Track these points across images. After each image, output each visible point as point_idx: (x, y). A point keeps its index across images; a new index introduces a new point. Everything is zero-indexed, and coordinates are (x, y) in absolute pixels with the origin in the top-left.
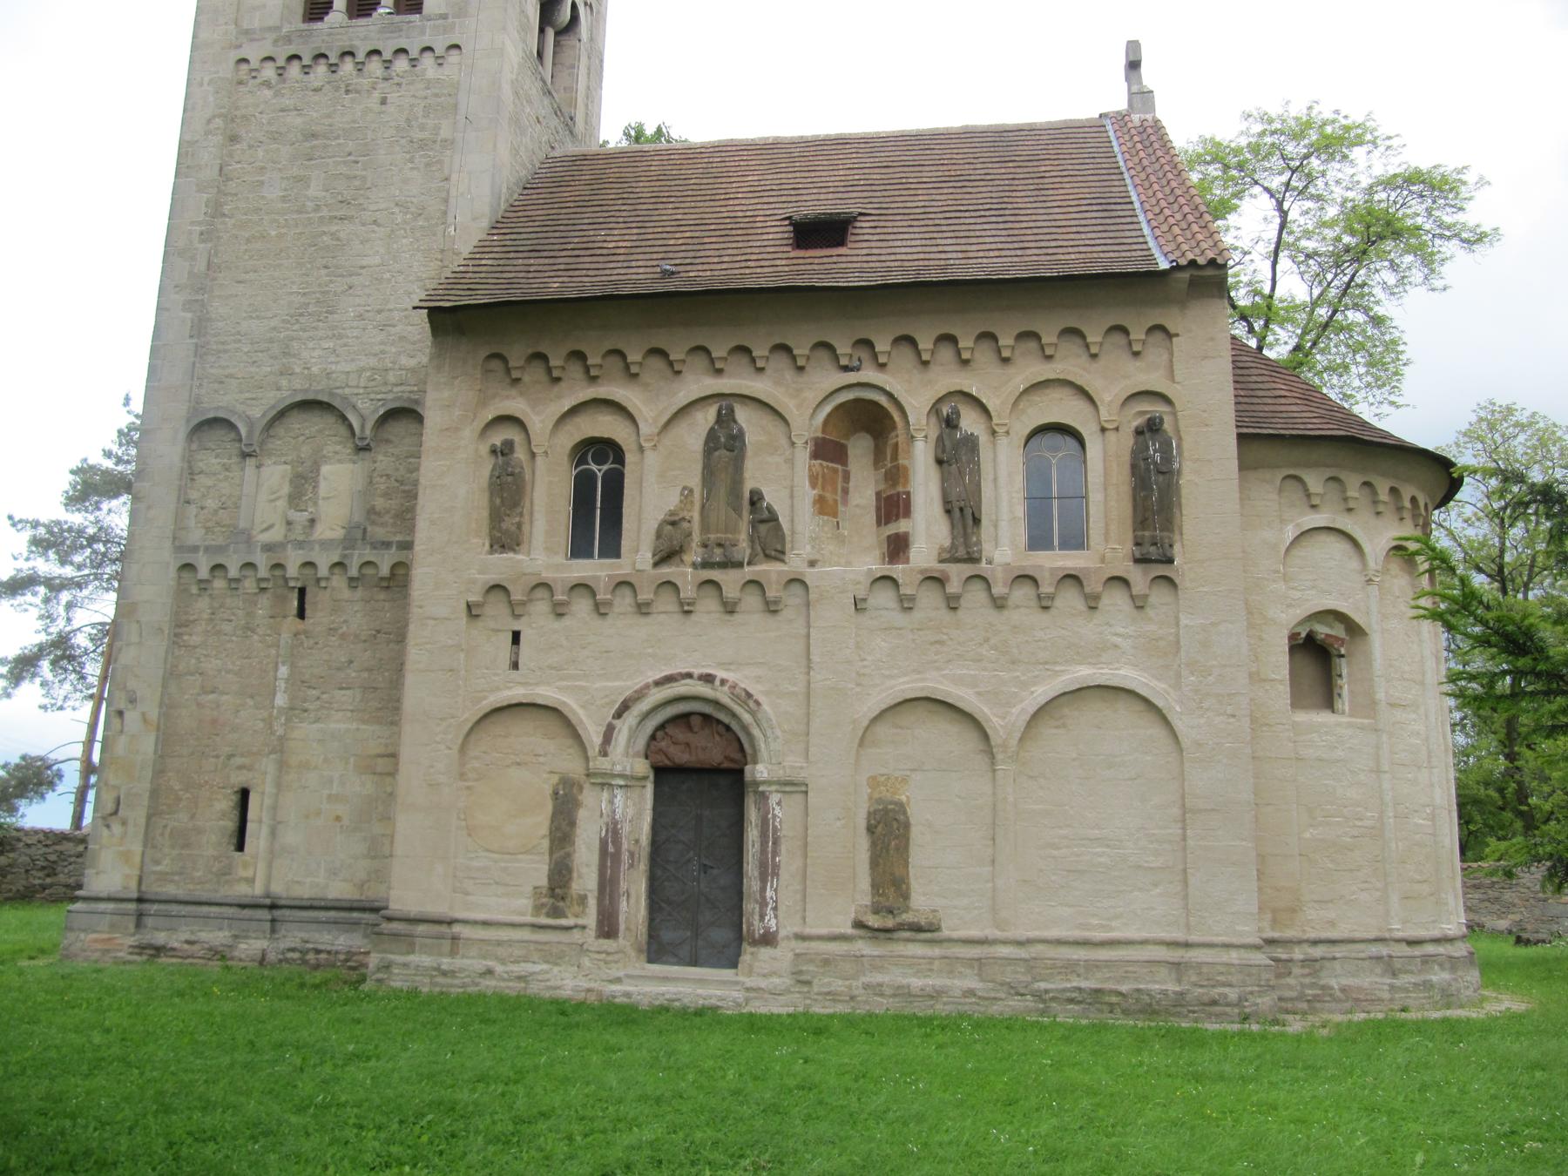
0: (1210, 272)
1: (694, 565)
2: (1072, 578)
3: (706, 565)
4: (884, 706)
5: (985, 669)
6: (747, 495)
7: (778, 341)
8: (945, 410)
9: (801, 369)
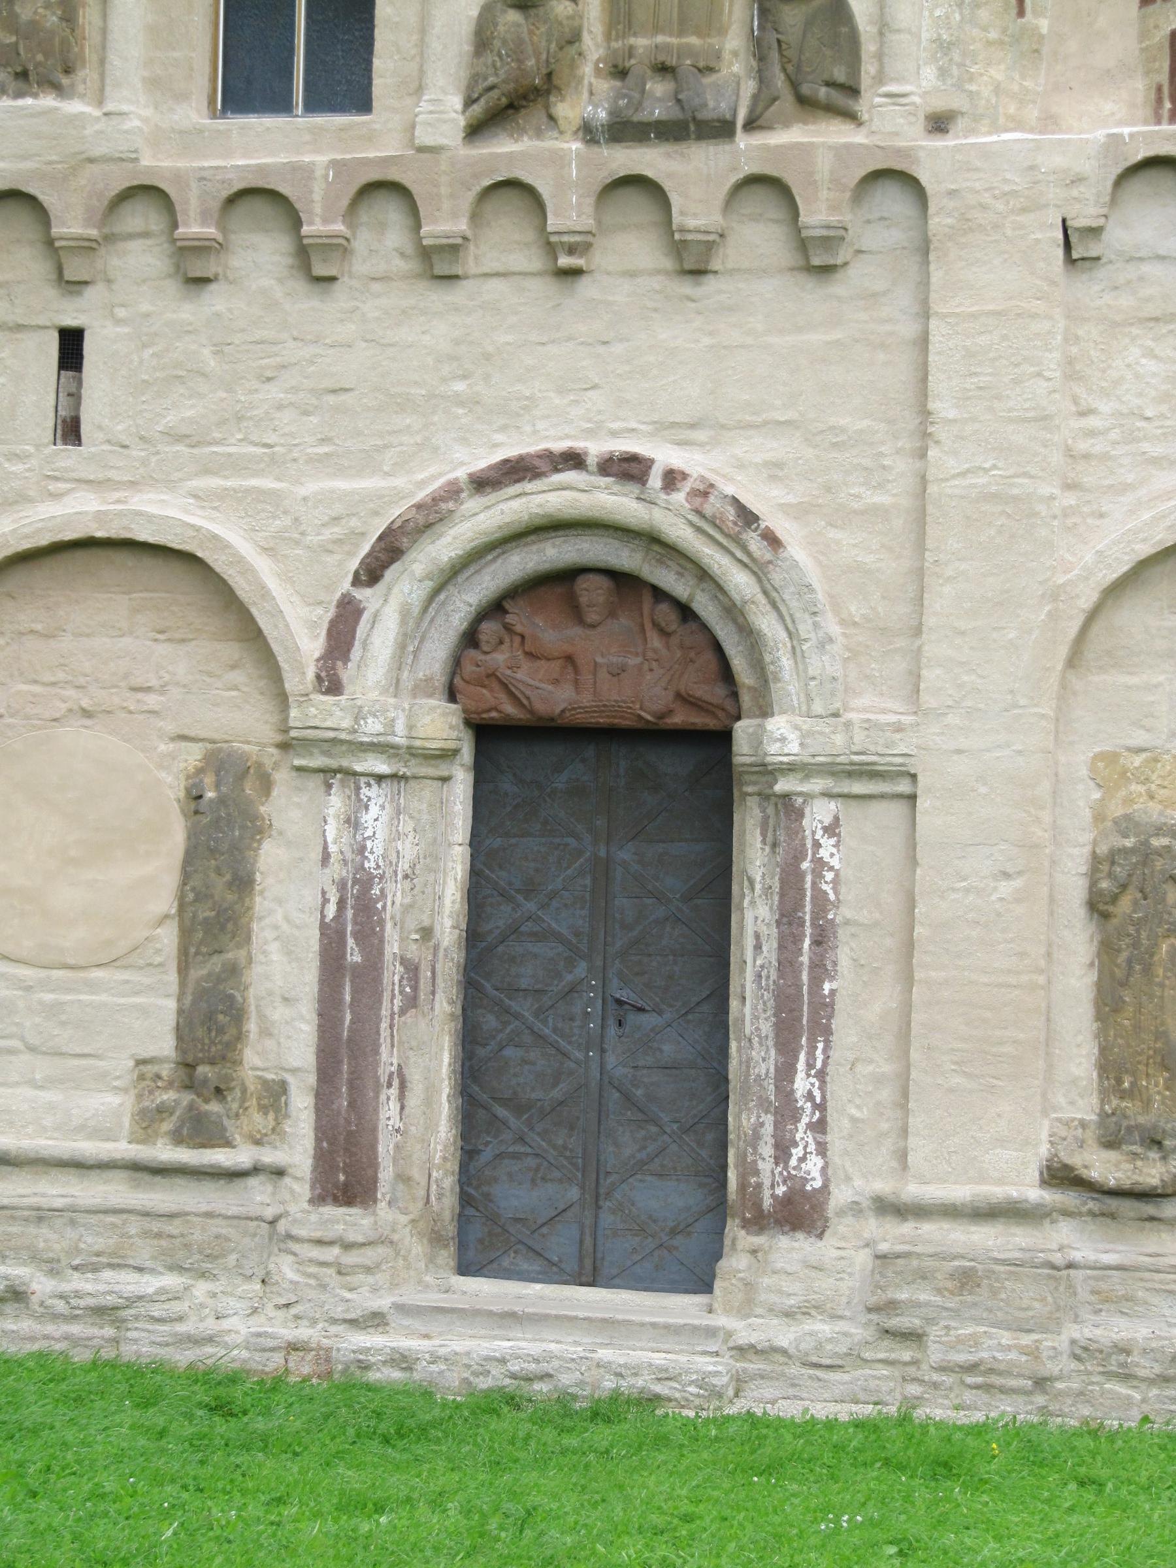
1: (588, 132)
3: (623, 130)
4: (1145, 550)
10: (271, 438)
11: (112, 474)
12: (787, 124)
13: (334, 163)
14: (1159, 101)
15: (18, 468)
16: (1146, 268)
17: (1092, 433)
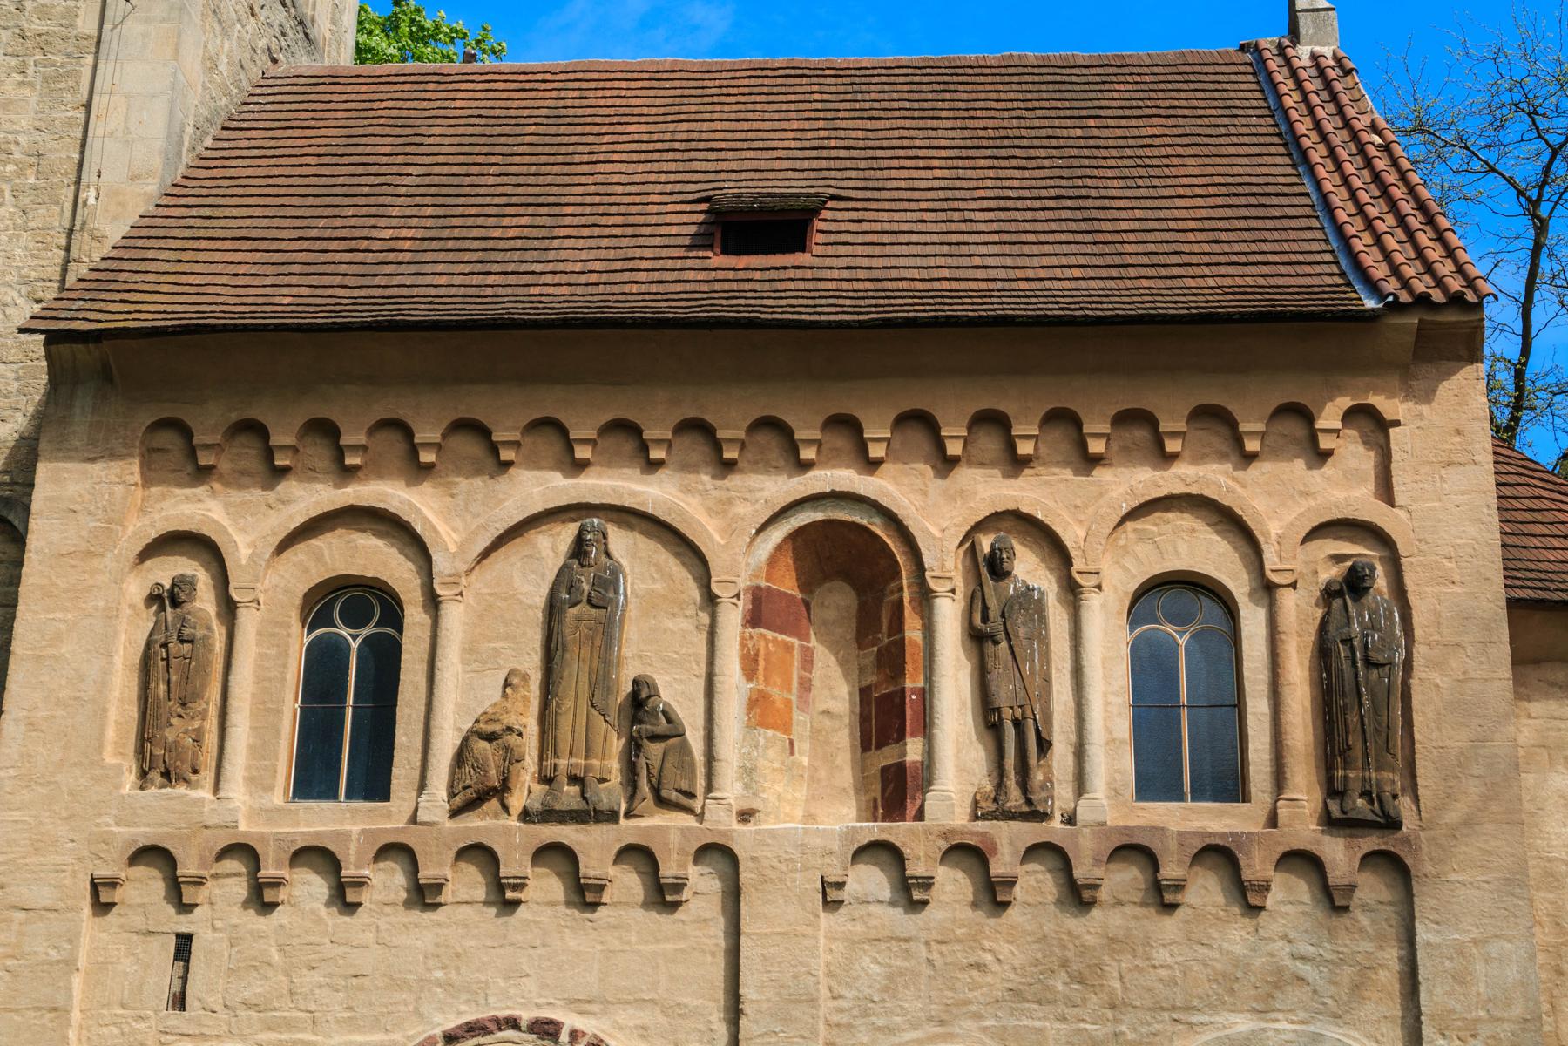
0: (1451, 317)
1: (525, 816)
2: (1219, 855)
3: (549, 815)
5: (1063, 1019)
6: (627, 688)
7: (692, 413)
8: (986, 543)
9: (728, 467)
10: (312, 1007)
11: (206, 1031)
12: (652, 815)
13: (363, 831)
14: (875, 808)
15: (141, 1026)
16: (873, 908)
17: (841, 1010)
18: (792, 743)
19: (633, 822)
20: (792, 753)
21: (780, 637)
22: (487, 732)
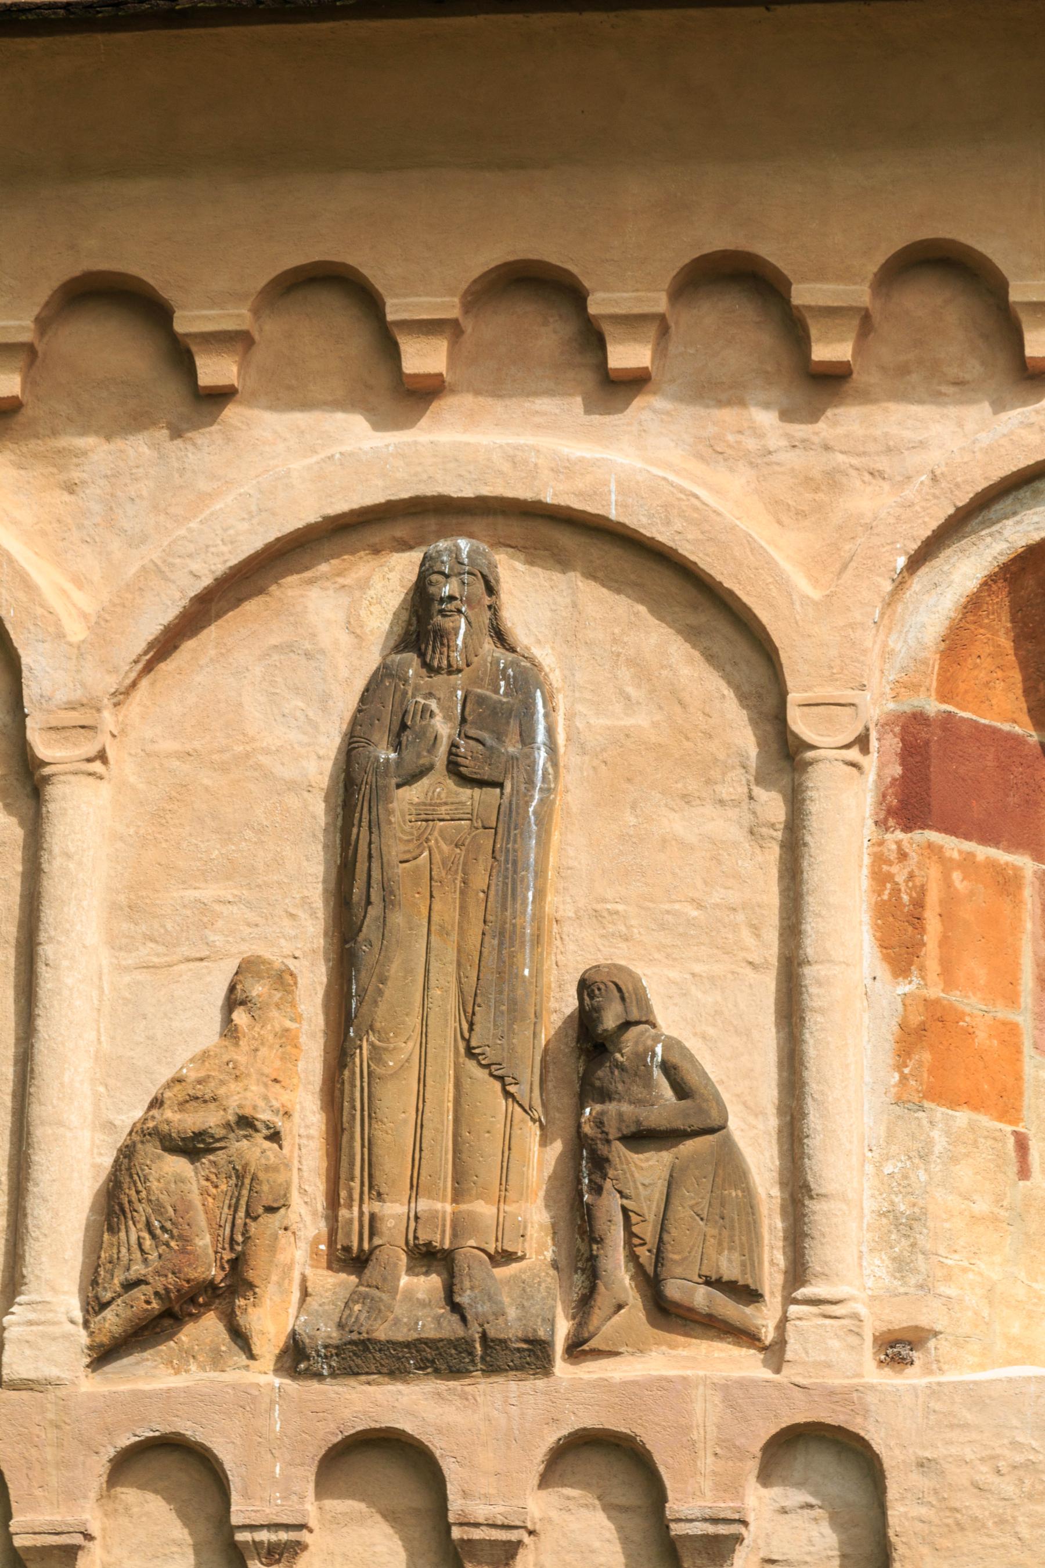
1: (296, 1357)
3: (359, 1355)
7: (719, 238)
9: (828, 383)
12: (641, 1350)
18: (1022, 1145)
19: (591, 1371)
20: (1024, 1172)
21: (983, 852)
22: (184, 1135)
